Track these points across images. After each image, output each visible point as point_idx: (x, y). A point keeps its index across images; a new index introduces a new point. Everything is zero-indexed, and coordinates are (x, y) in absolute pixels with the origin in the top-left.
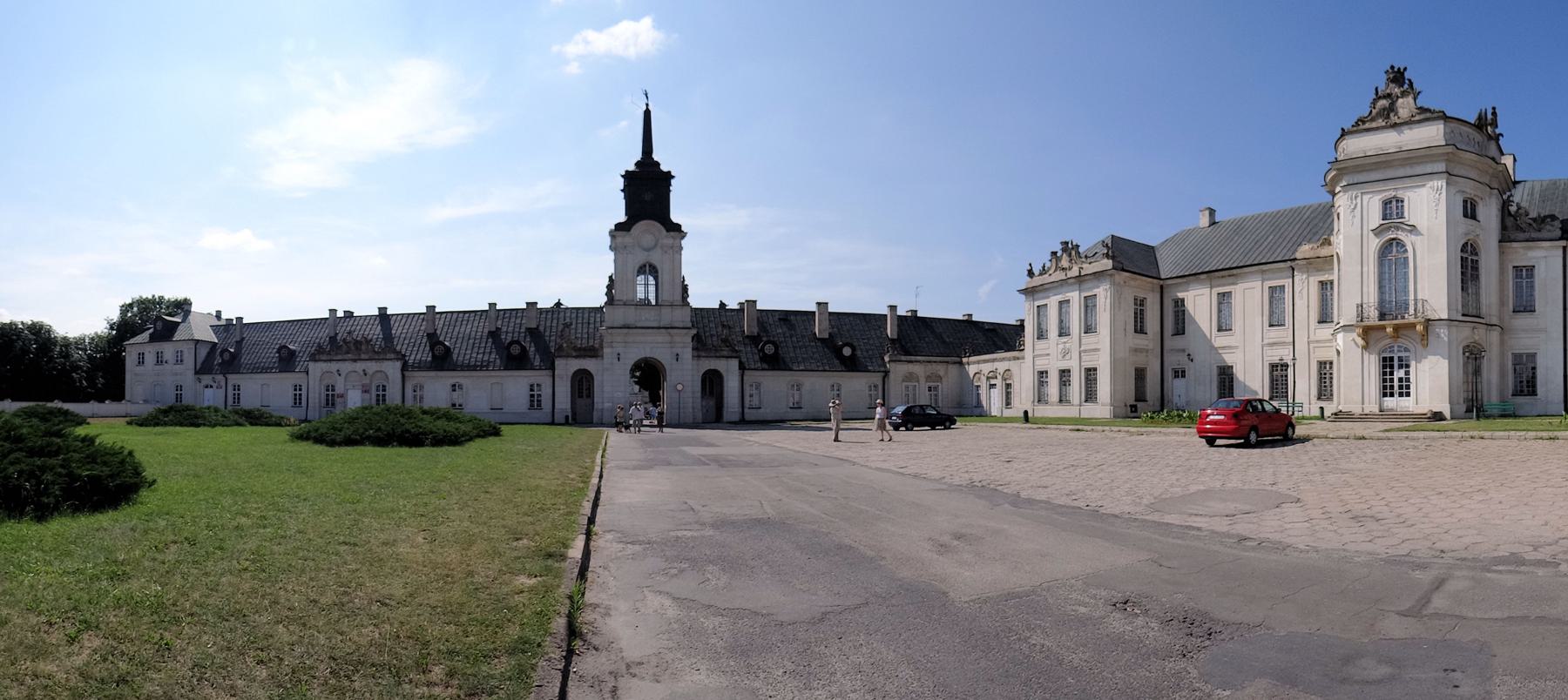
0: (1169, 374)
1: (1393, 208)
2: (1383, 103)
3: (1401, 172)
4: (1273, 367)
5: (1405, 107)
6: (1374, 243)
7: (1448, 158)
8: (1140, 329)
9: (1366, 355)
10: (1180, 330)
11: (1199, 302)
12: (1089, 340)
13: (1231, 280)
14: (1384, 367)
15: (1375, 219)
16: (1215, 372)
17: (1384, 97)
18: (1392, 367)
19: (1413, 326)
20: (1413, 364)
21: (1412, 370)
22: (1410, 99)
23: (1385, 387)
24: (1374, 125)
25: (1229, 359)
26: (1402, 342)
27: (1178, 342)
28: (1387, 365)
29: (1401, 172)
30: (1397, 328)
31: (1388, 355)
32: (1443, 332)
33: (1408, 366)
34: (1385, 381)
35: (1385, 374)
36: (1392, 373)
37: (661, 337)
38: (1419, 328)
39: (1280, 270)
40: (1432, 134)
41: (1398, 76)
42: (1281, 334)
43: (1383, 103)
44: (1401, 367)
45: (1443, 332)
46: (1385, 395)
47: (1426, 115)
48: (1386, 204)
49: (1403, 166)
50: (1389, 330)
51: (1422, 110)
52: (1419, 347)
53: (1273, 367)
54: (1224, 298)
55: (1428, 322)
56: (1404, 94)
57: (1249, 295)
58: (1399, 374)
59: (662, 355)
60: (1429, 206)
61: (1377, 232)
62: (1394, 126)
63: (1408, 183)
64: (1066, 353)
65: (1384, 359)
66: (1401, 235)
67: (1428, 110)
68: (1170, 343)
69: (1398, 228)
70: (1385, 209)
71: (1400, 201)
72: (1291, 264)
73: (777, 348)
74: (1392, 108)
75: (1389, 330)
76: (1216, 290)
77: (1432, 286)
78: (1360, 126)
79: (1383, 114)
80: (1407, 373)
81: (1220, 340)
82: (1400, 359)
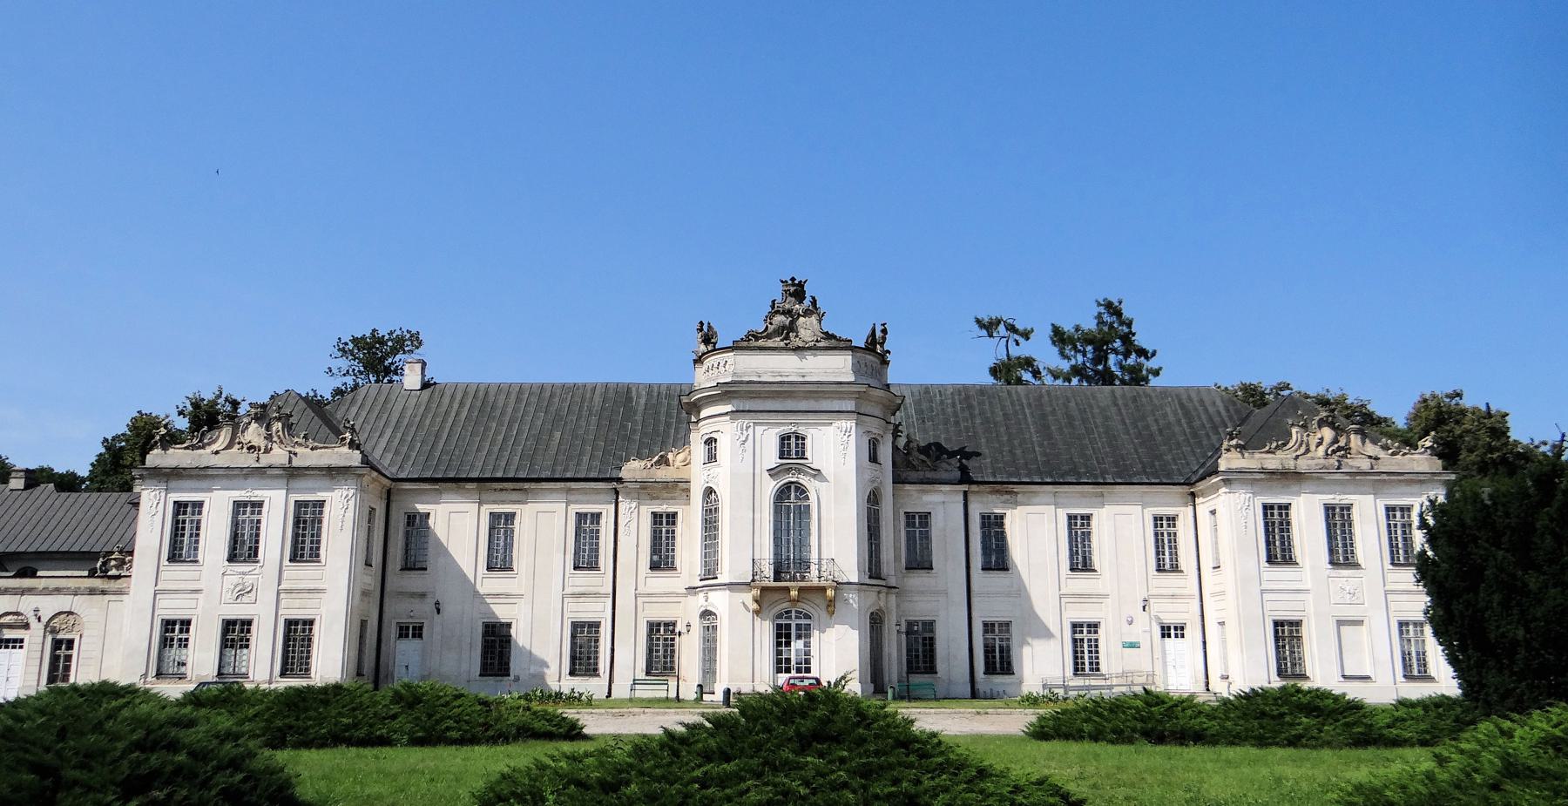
0: (391, 631)
1: (792, 447)
2: (779, 319)
3: (803, 405)
4: (576, 626)
5: (807, 329)
6: (770, 487)
7: (859, 397)
8: (368, 564)
9: (758, 621)
10: (413, 564)
11: (457, 524)
12: (301, 574)
13: (515, 496)
14: (779, 636)
15: (772, 458)
16: (480, 630)
17: (784, 313)
18: (788, 636)
19: (823, 589)
20: (816, 633)
21: (814, 641)
22: (814, 319)
23: (779, 662)
24: (770, 343)
25: (502, 613)
26: (805, 607)
27: (413, 581)
28: (783, 636)
29: (803, 405)
30: (801, 590)
31: (783, 621)
32: (853, 598)
33: (808, 636)
34: (779, 653)
35: (779, 644)
36: (788, 644)
38: (830, 593)
39: (598, 492)
40: (838, 367)
41: (798, 291)
42: (599, 581)
43: (779, 319)
44: (799, 637)
45: (853, 598)
46: (779, 670)
47: (833, 343)
48: (784, 439)
49: (806, 398)
50: (794, 593)
51: (828, 336)
52: (824, 614)
53: (576, 626)
54: (501, 525)
55: (839, 586)
56: (807, 313)
57: (544, 523)
58: (797, 645)
60: (835, 449)
61: (773, 473)
62: (797, 349)
63: (811, 418)
64: (242, 593)
65: (779, 627)
66: (804, 480)
67: (833, 337)
68: (397, 581)
69: (799, 471)
70: (782, 445)
71: (801, 438)
72: (615, 486)
74: (791, 328)
75: (794, 593)
76: (487, 509)
77: (837, 547)
78: (749, 343)
79: (779, 332)
80: (807, 645)
81: (489, 584)
82: (798, 627)
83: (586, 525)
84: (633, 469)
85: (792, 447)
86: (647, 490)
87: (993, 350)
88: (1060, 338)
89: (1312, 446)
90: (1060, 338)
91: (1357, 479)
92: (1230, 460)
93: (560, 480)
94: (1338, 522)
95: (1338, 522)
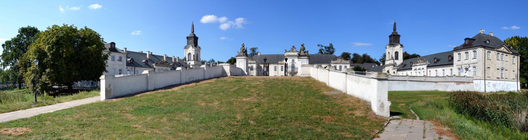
1: (293, 61)
5: (294, 50)
72: (278, 64)
78: (289, 51)
79: (292, 51)
83: (275, 68)
84: (279, 62)
85: (293, 61)
86: (281, 64)
87: (319, 48)
88: (325, 47)
89: (339, 60)
90: (325, 47)
91: (342, 63)
92: (332, 62)
93: (273, 63)
94: (340, 67)
95: (340, 67)
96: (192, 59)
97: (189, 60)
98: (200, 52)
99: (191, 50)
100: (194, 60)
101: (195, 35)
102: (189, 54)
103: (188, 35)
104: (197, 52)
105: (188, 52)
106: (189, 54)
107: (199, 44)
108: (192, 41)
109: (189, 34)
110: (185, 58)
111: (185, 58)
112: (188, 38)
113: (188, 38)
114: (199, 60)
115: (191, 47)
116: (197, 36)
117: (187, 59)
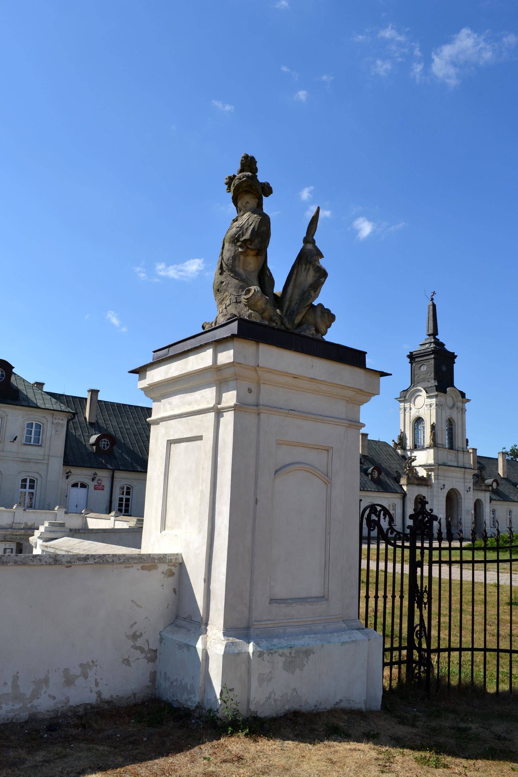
37: (458, 474)
59: (460, 488)
73: (498, 485)
96: (428, 441)
97: (416, 447)
98: (463, 411)
99: (425, 406)
100: (435, 444)
101: (440, 345)
102: (419, 420)
103: (416, 348)
104: (447, 414)
105: (414, 413)
106: (419, 420)
107: (459, 382)
108: (427, 368)
109: (418, 340)
110: (402, 438)
111: (402, 438)
112: (412, 357)
113: (412, 357)
114: (459, 443)
115: (424, 393)
116: (449, 348)
117: (409, 443)
